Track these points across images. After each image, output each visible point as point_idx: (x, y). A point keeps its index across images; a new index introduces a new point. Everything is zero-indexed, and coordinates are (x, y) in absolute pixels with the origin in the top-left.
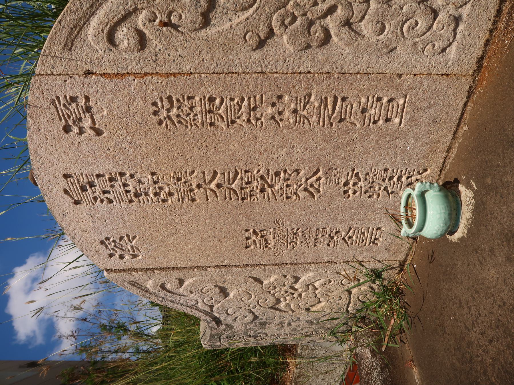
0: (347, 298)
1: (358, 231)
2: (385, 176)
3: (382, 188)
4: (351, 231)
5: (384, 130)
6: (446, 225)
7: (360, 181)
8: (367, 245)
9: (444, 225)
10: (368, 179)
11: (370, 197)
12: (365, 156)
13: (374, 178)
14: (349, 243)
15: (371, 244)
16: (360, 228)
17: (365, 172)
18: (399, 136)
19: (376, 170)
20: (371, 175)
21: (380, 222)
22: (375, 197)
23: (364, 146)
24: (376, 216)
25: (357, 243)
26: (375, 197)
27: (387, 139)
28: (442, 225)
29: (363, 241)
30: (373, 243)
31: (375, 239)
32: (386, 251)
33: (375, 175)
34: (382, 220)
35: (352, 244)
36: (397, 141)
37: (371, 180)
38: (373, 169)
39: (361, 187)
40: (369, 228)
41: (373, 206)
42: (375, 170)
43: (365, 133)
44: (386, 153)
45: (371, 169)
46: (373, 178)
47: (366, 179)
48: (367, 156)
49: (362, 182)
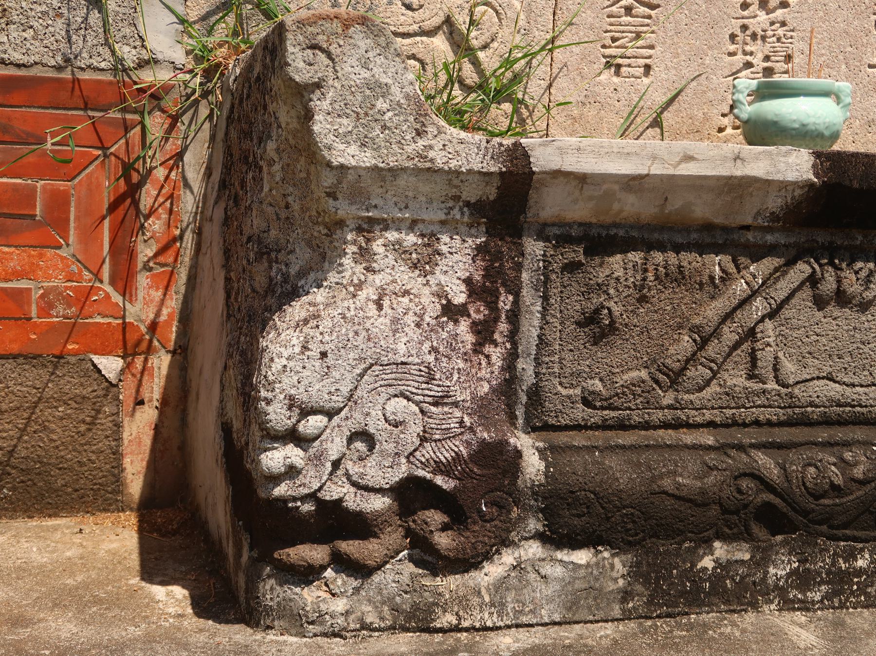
0: (415, 27)
1: (648, 25)
2: (777, 58)
3: (748, 58)
4: (646, 9)
5: (865, 41)
6: (827, 128)
7: (767, 14)
8: (602, 50)
9: (827, 125)
10: (773, 27)
11: (733, 37)
12: (821, 14)
13: (774, 39)
14: (614, 8)
15: (605, 61)
16: (654, 28)
17: (788, 19)
18: (852, 68)
19: (790, 40)
20: (781, 32)
21: (667, 68)
22: (732, 48)
23: (840, 11)
24: (683, 58)
25: (612, 28)
26: (732, 48)
27: (849, 49)
28: (827, 120)
29: (614, 40)
30: (608, 65)
31: (619, 66)
32: (582, 98)
33: (779, 40)
34: (674, 72)
35: (608, 17)
36: (844, 67)
37: (770, 33)
38: (792, 33)
39: (755, 17)
40: (652, 47)
41: (711, 48)
42: (791, 37)
43: (863, 7)
44: (823, 52)
45: (793, 31)
46: (774, 35)
47: (772, 23)
48: (821, 18)
49: (766, 17)
